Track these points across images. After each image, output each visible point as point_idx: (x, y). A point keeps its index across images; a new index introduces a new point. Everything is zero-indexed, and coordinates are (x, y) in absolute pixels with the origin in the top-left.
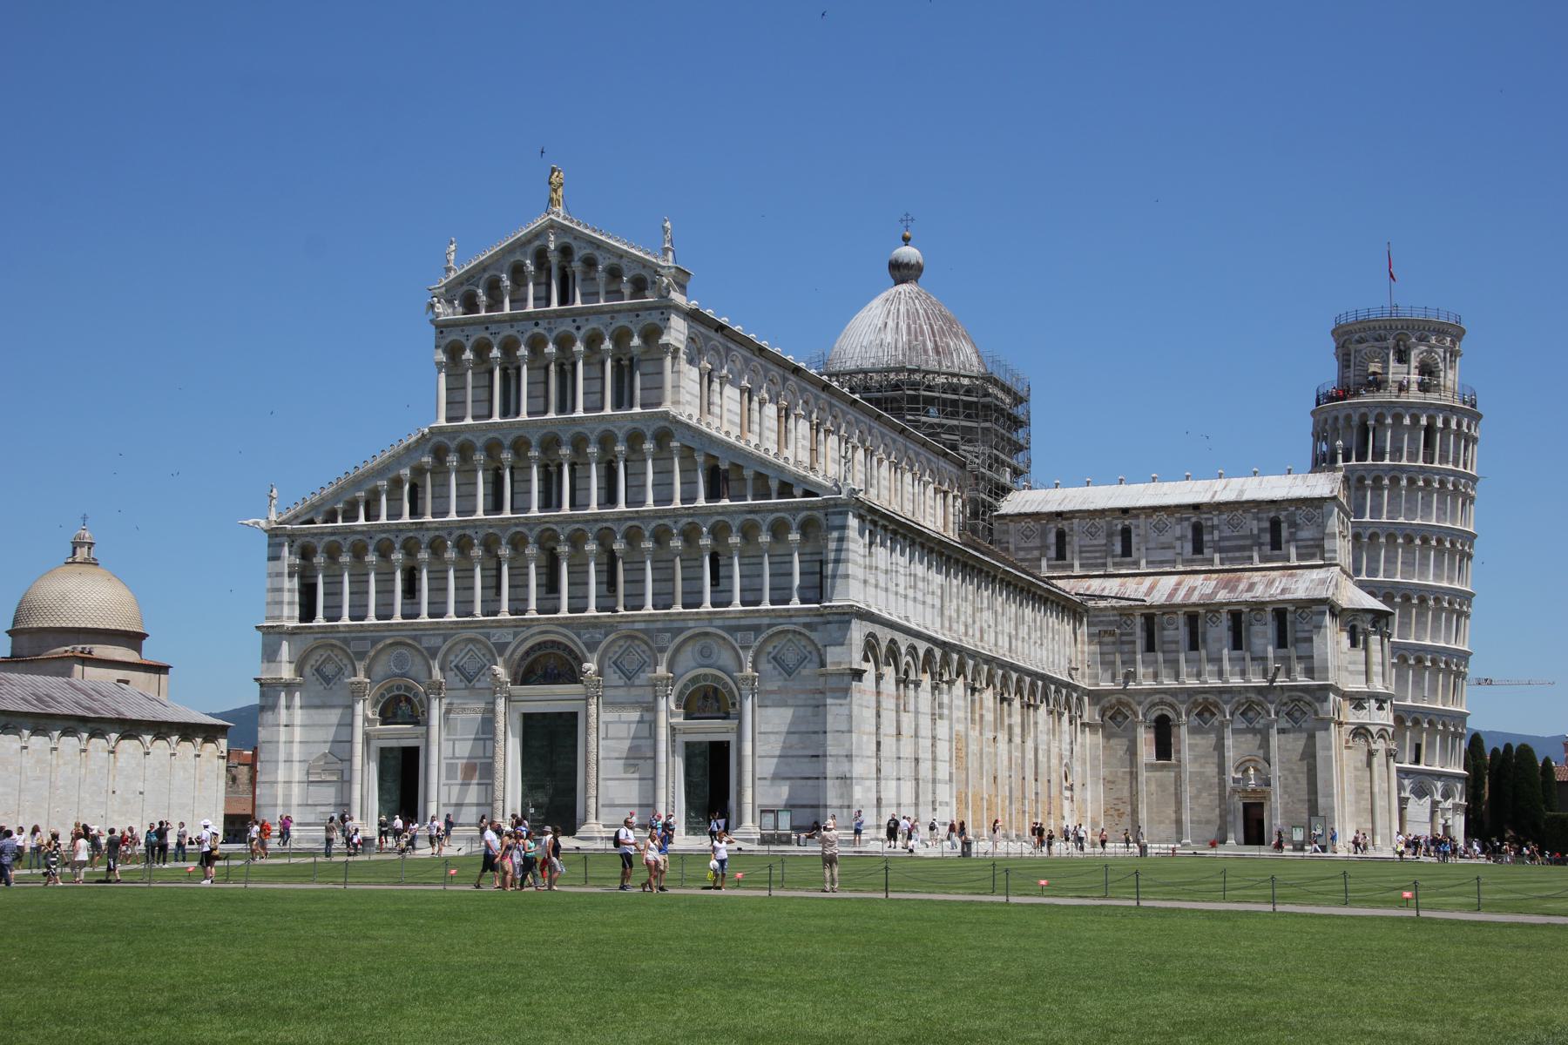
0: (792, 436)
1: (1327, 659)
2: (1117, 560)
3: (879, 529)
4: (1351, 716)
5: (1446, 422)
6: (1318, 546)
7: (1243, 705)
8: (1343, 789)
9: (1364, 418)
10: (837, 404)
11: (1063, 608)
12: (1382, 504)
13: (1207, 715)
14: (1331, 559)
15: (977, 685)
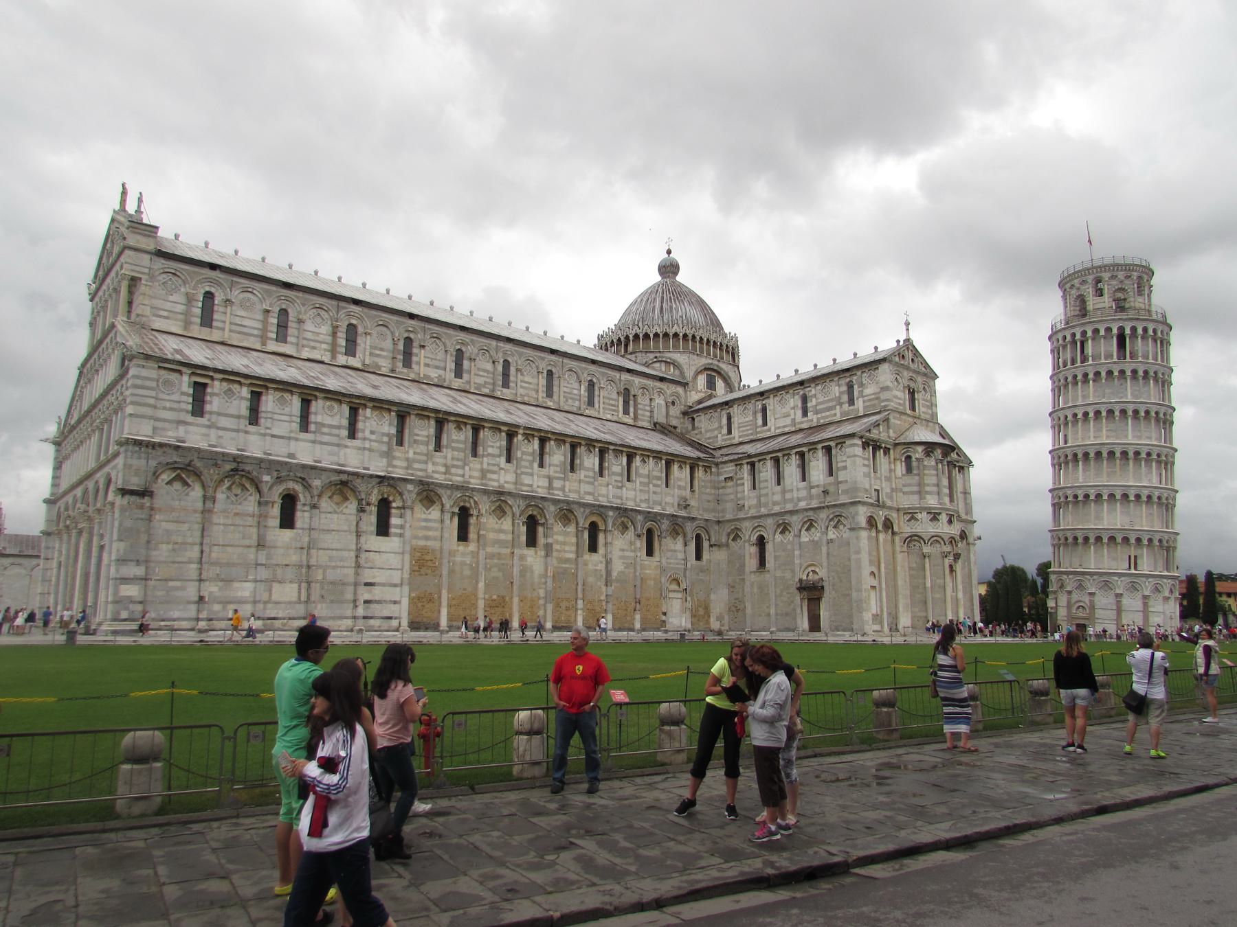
0: (359, 349)
1: (856, 482)
2: (758, 430)
3: (217, 383)
4: (905, 528)
5: (1134, 329)
6: (877, 398)
7: (805, 523)
8: (895, 586)
9: (1074, 335)
10: (437, 329)
11: (668, 464)
12: (1089, 392)
13: (787, 533)
14: (885, 406)
15: (475, 513)
